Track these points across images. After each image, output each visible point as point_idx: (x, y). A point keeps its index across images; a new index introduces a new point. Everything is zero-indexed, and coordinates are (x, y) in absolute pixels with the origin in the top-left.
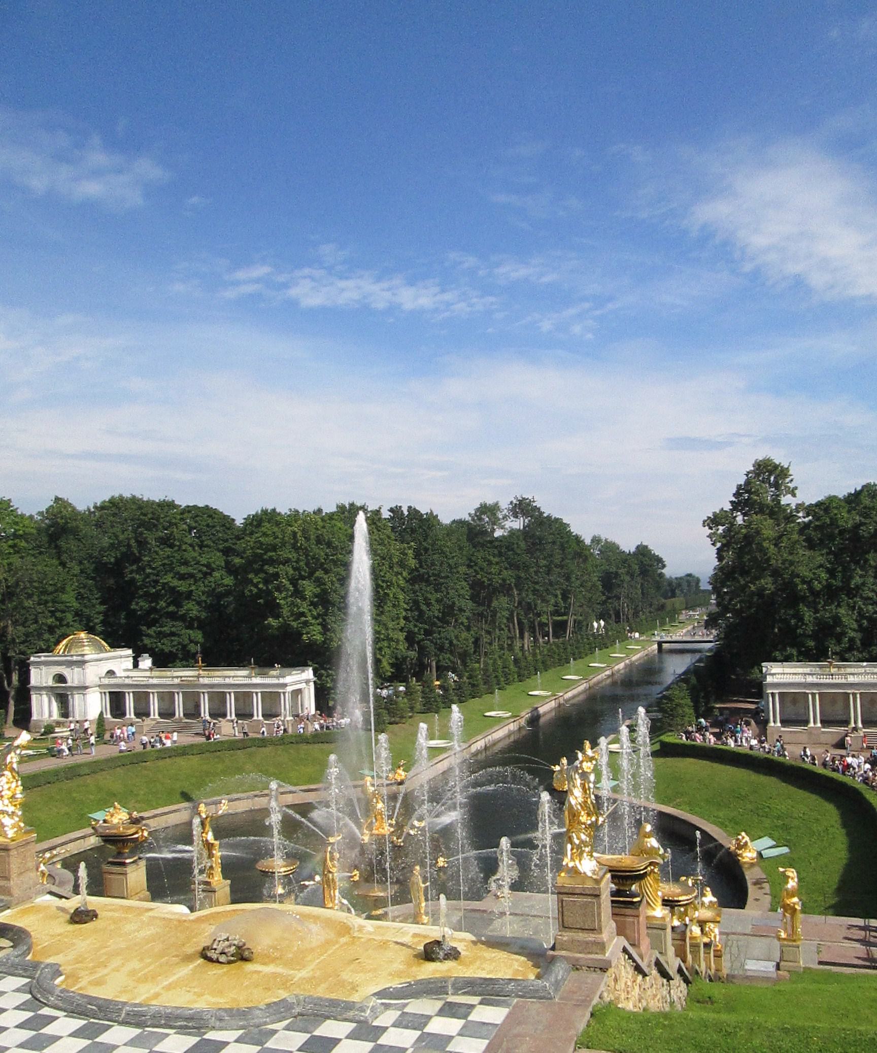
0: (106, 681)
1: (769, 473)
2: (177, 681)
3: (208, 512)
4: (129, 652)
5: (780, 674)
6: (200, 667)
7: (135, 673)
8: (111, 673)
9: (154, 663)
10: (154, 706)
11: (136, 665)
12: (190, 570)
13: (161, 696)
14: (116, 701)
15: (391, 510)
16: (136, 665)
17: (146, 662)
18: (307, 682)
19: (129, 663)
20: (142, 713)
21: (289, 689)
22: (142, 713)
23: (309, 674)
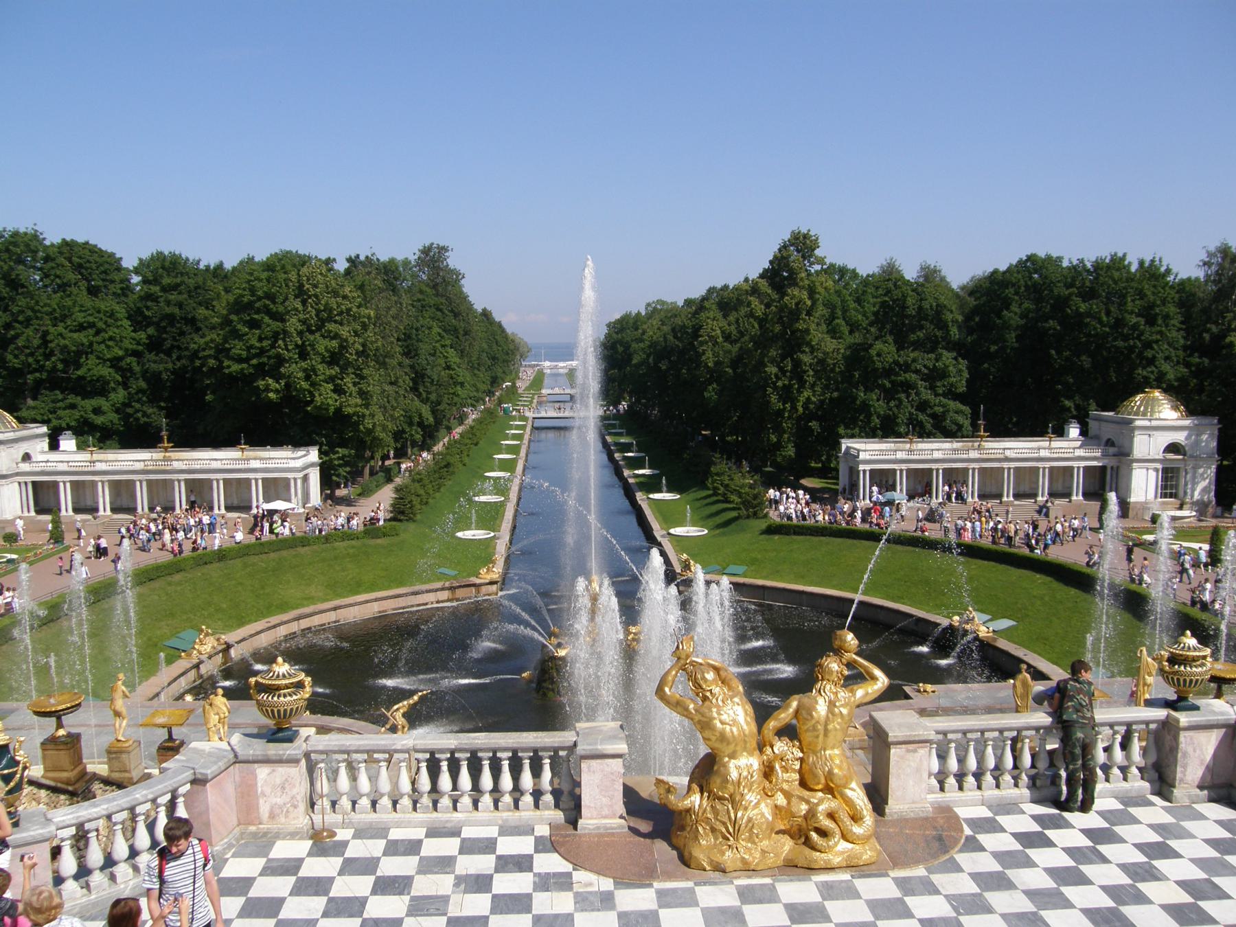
0: (25, 467)
1: (803, 244)
2: (139, 466)
3: (93, 250)
4: (44, 429)
5: (869, 452)
6: (166, 449)
7: (54, 456)
8: (27, 457)
9: (81, 447)
10: (104, 500)
11: (54, 446)
12: (91, 319)
13: (76, 486)
14: (43, 496)
15: (349, 260)
16: (54, 446)
17: (68, 443)
18: (312, 465)
19: (45, 444)
20: (85, 507)
21: (301, 475)
22: (85, 507)
23: (313, 455)
